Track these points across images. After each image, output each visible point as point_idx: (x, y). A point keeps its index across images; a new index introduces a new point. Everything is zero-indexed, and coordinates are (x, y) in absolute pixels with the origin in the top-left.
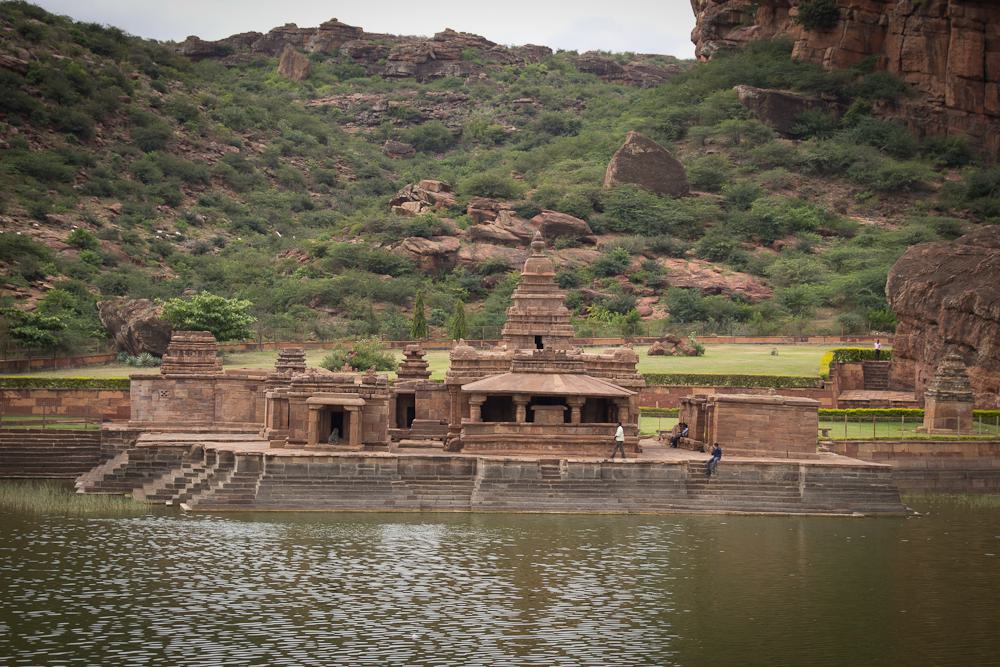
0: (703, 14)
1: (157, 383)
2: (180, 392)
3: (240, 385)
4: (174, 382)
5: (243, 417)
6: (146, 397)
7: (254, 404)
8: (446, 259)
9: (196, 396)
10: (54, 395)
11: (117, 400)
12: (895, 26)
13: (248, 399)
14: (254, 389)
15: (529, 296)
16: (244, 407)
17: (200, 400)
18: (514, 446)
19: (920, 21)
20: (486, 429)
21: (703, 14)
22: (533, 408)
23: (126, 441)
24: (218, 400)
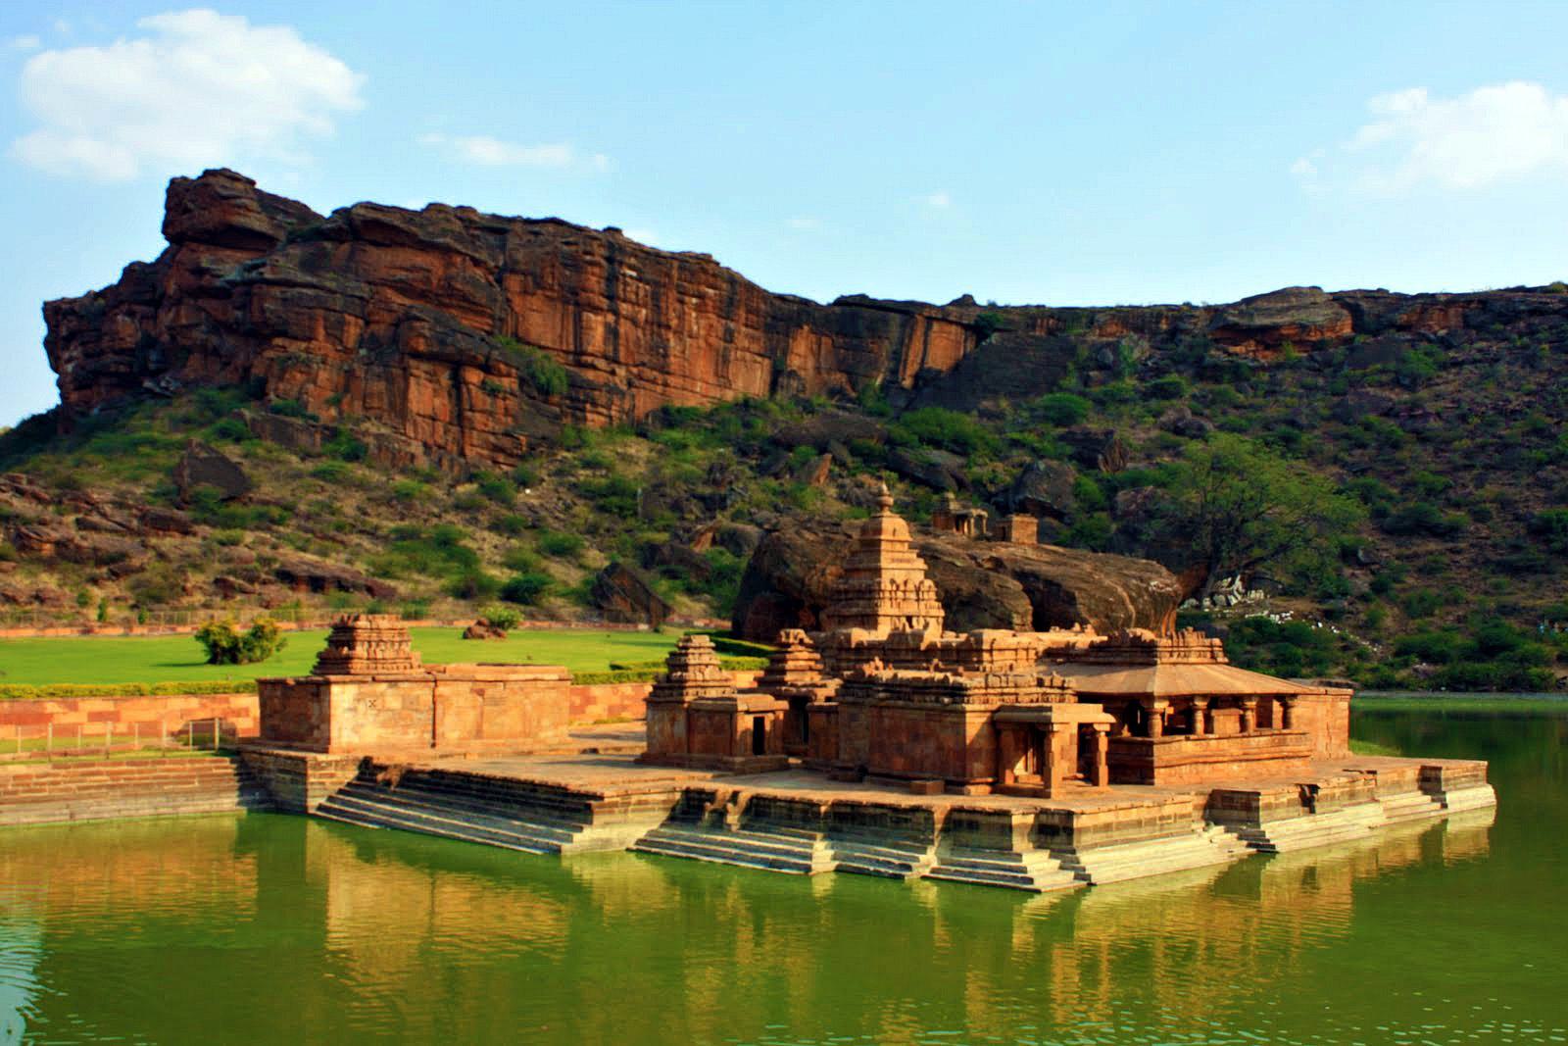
0: (70, 368)
1: (366, 688)
2: (393, 699)
3: (466, 687)
4: (384, 686)
5: (469, 732)
6: (350, 709)
7: (482, 714)
8: (66, 546)
9: (410, 704)
10: (107, 706)
11: (189, 711)
12: (360, 371)
13: (474, 707)
14: (481, 693)
15: (894, 565)
16: (471, 717)
17: (417, 710)
18: (1200, 767)
19: (381, 369)
20: (1175, 745)
21: (70, 368)
22: (1214, 713)
23: (339, 773)
24: (439, 711)
